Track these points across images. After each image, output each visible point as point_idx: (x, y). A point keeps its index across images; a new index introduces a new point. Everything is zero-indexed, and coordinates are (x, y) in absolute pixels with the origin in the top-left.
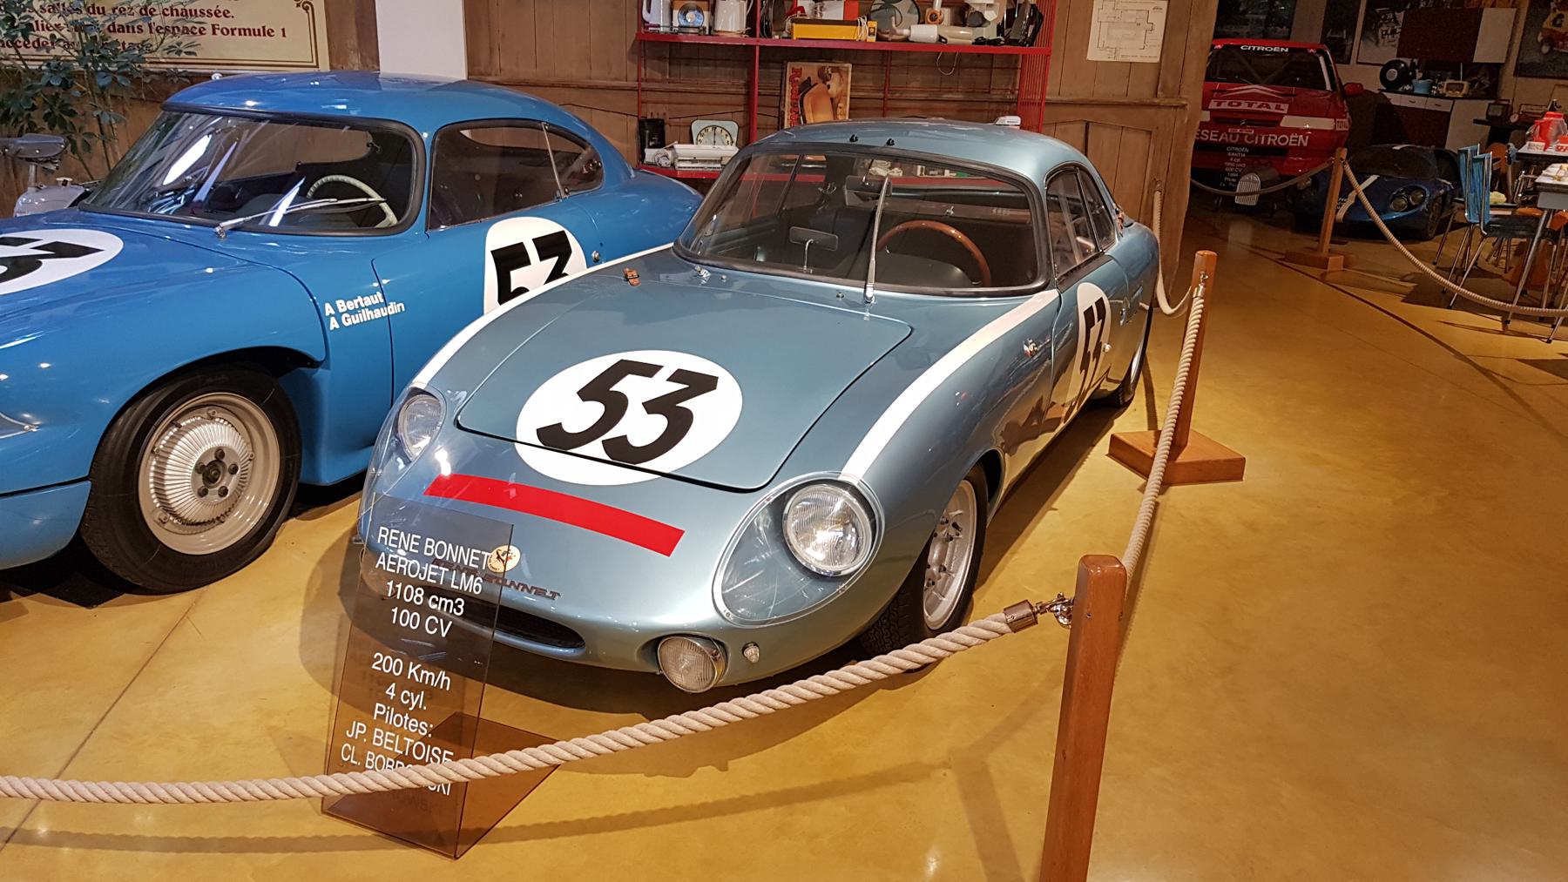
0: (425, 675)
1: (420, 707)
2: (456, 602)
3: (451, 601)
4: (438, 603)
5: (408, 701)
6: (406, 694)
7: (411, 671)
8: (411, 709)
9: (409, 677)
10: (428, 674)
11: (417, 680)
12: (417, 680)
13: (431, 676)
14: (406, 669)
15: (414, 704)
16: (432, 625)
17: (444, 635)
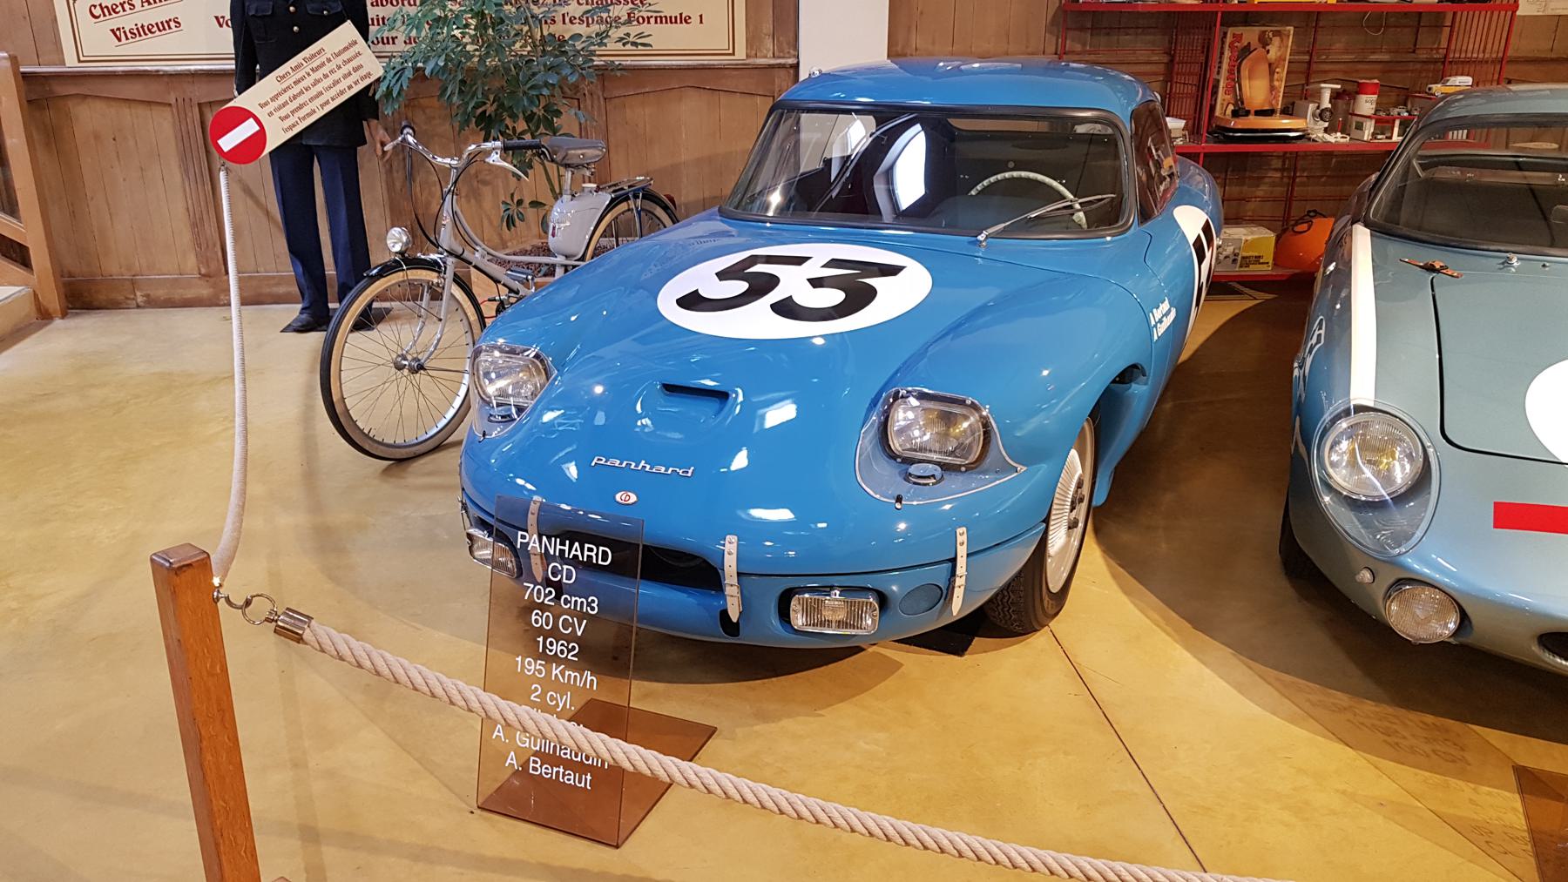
0: (570, 675)
1: (568, 707)
3: (583, 600)
5: (554, 702)
6: (552, 695)
7: (554, 673)
8: (559, 710)
9: (553, 678)
10: (573, 675)
11: (562, 681)
12: (562, 681)
13: (575, 676)
14: (549, 672)
15: (561, 705)
16: (566, 624)
17: (579, 634)
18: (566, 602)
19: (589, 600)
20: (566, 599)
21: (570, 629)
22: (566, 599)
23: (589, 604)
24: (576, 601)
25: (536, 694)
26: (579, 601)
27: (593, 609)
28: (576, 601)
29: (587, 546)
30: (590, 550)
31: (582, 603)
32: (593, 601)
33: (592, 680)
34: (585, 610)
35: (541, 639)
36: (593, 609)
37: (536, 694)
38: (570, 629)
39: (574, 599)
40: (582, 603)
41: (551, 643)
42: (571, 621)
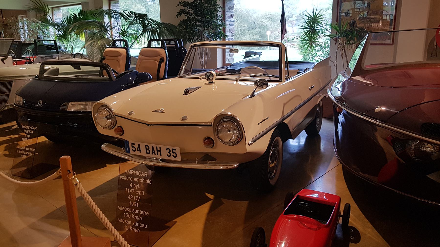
2: (142, 192)
4: (138, 193)
18: (137, 192)
19: (142, 192)
20: (137, 192)
21: (137, 199)
22: (137, 192)
23: (142, 193)
24: (139, 192)
25: (132, 198)
26: (140, 192)
27: (143, 194)
28: (139, 192)
29: (145, 172)
30: (146, 174)
31: (140, 192)
32: (143, 192)
33: (141, 218)
34: (141, 194)
35: (130, 202)
36: (143, 194)
37: (132, 198)
38: (137, 199)
39: (138, 192)
40: (140, 192)
41: (133, 203)
42: (137, 197)
